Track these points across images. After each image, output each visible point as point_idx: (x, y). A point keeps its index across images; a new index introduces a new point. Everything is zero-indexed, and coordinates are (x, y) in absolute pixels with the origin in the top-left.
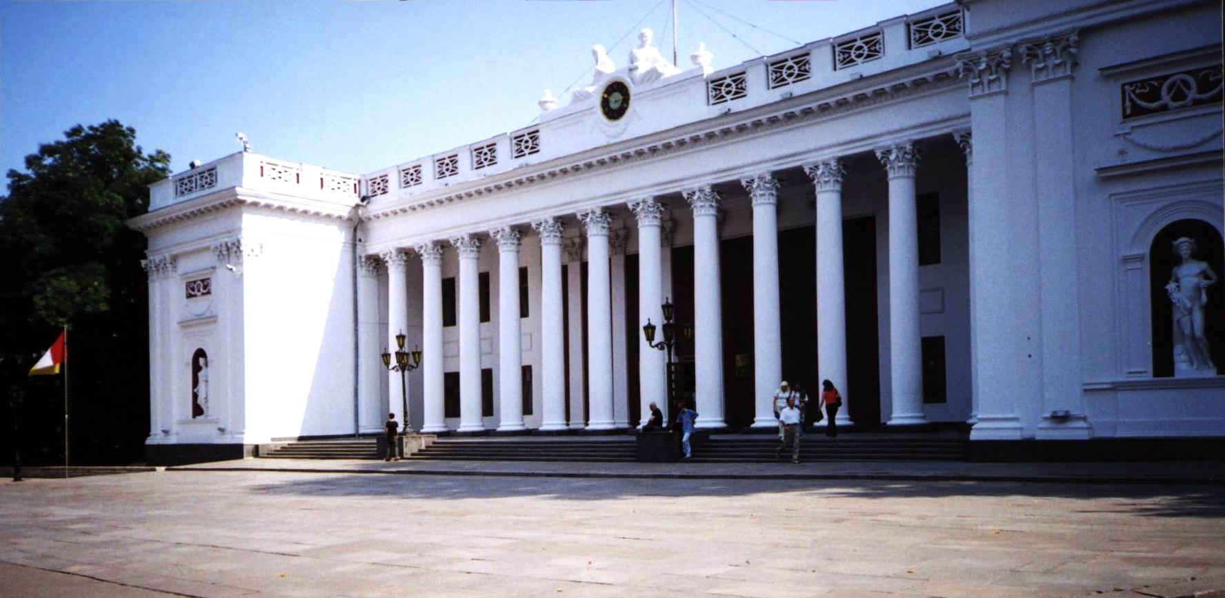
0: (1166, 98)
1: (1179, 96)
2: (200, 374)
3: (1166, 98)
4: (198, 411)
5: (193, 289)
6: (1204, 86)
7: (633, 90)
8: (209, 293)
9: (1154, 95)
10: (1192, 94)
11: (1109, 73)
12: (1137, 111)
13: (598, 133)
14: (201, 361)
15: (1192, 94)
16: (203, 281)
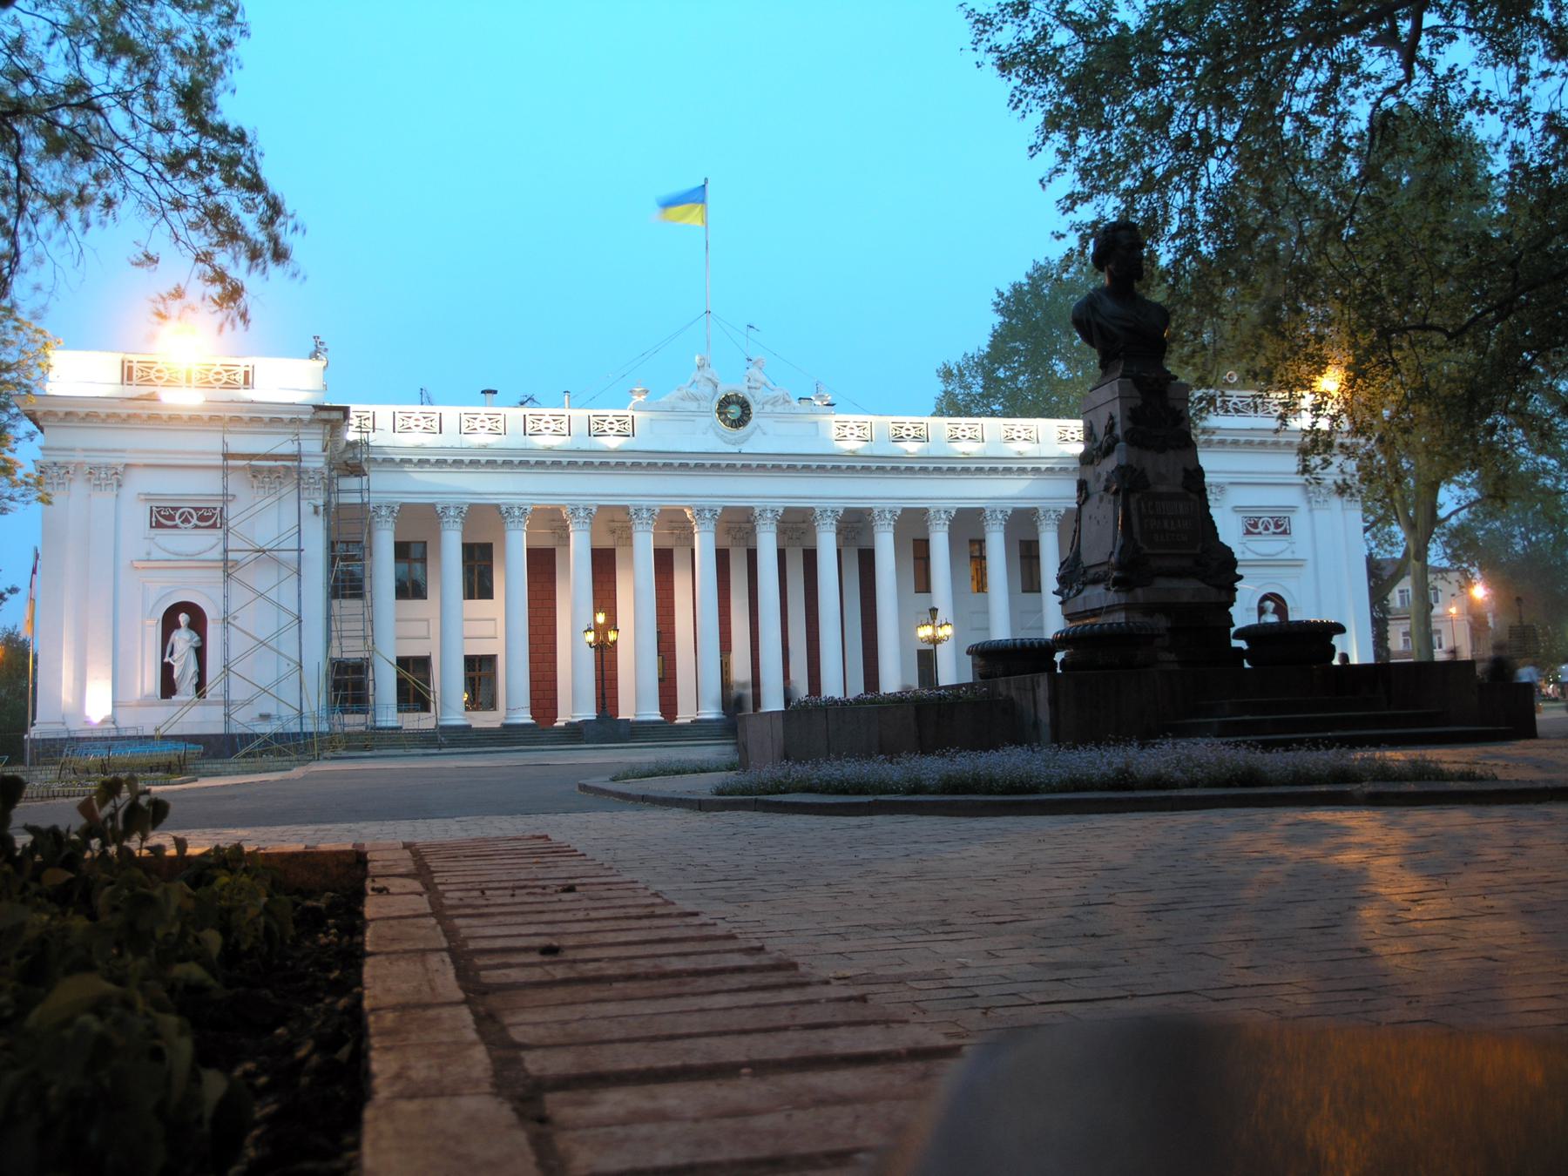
0: (1261, 528)
1: (1266, 529)
2: (183, 639)
3: (1261, 528)
4: (168, 686)
5: (171, 518)
6: (1277, 526)
7: (754, 409)
8: (214, 526)
9: (1255, 526)
10: (1272, 529)
11: (1236, 509)
12: (1248, 533)
13: (708, 436)
14: (183, 618)
15: (1272, 529)
16: (196, 509)
